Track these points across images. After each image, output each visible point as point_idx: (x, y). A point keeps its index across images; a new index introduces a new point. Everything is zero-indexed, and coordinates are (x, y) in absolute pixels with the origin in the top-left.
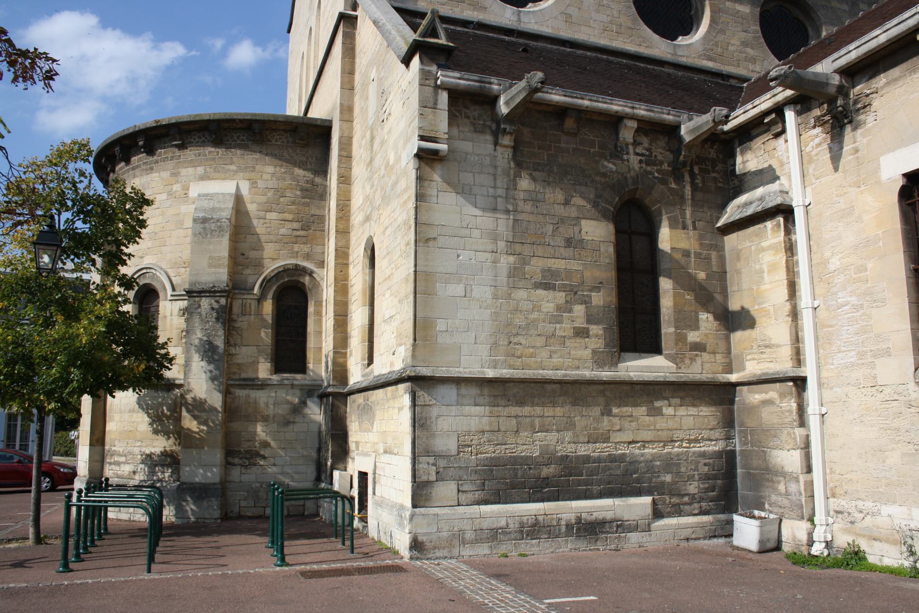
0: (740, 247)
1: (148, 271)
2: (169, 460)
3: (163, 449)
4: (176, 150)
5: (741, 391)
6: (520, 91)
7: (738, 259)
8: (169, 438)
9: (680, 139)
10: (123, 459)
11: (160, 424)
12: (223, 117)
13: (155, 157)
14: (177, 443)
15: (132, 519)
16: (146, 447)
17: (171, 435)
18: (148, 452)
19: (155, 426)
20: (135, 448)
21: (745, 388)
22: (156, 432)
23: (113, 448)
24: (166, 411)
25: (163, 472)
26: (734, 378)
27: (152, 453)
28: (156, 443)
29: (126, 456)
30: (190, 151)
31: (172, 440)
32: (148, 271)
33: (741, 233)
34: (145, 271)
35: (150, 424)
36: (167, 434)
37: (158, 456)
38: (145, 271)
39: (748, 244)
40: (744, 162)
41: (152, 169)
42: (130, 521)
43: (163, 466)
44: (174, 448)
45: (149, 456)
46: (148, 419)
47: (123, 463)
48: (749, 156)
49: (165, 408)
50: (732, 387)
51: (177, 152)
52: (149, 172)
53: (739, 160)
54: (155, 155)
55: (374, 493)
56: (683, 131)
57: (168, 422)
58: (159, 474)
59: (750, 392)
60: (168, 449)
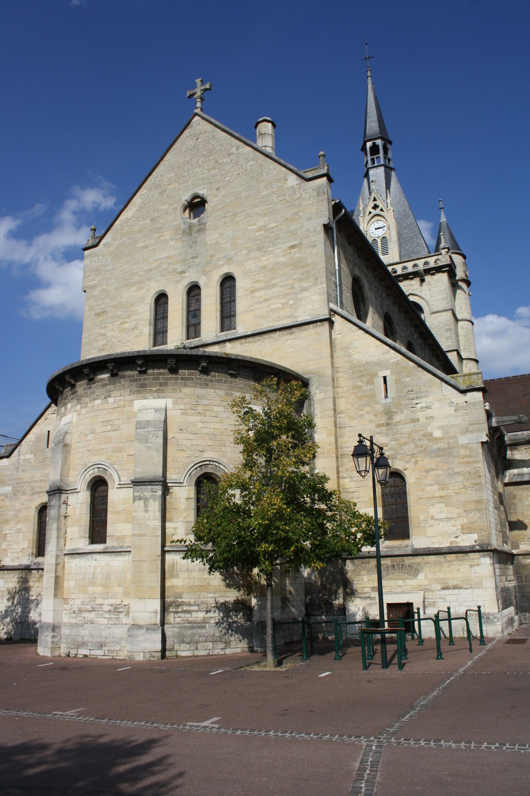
0: (515, 493)
1: (211, 463)
2: (240, 606)
3: (235, 599)
4: (229, 376)
5: (518, 558)
6: (511, 421)
7: (514, 498)
8: (239, 591)
9: (504, 441)
10: (196, 608)
11: (232, 580)
12: (267, 364)
13: (209, 377)
14: (246, 594)
15: (211, 653)
16: (220, 597)
17: (241, 588)
18: (222, 600)
19: (228, 581)
20: (209, 599)
21: (521, 557)
22: (228, 586)
23: (180, 600)
24: (236, 570)
25: (236, 616)
26: (514, 552)
27: (226, 602)
28: (228, 594)
29: (198, 605)
30: (240, 380)
31: (242, 592)
32: (211, 463)
33: (516, 487)
34: (208, 463)
35: (222, 580)
36: (238, 587)
37: (232, 603)
38: (208, 463)
39: (521, 492)
40: (512, 455)
41: (207, 385)
42: (209, 655)
43: (236, 611)
44: (243, 597)
45: (224, 604)
46: (221, 577)
47: (194, 611)
48: (515, 452)
49: (235, 568)
50: (512, 556)
51: (229, 379)
52: (203, 386)
53: (509, 453)
54: (209, 375)
55: (424, 613)
56: (506, 438)
57: (238, 578)
58: (234, 617)
59: (523, 558)
60: (239, 598)
